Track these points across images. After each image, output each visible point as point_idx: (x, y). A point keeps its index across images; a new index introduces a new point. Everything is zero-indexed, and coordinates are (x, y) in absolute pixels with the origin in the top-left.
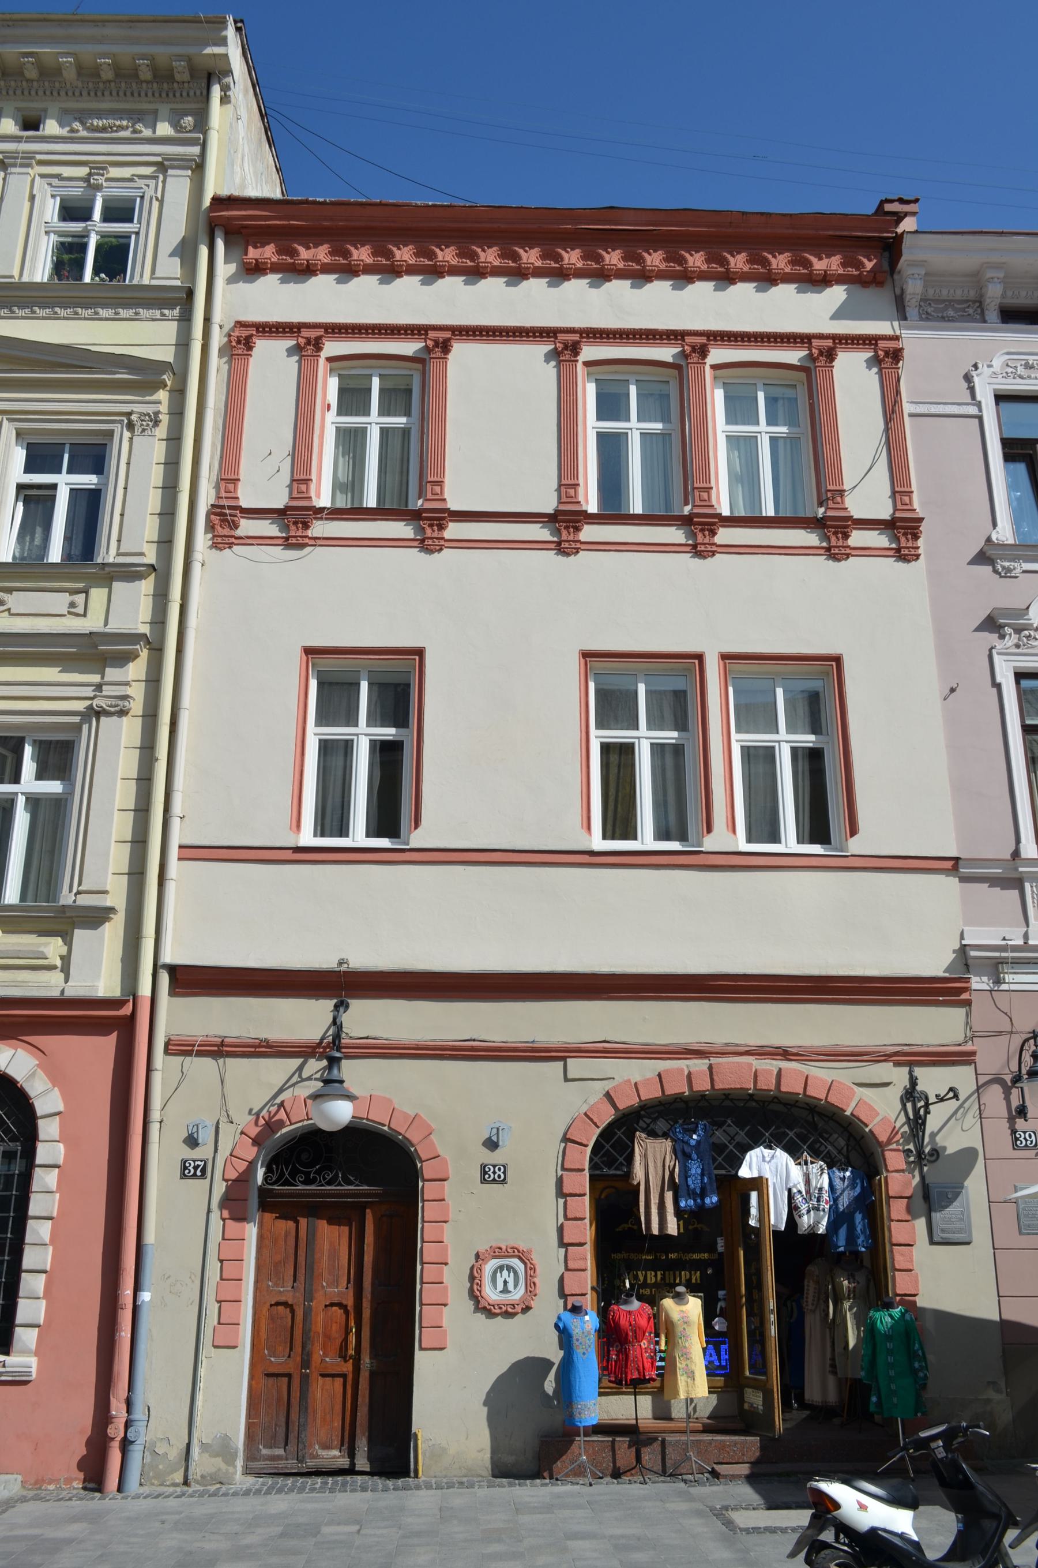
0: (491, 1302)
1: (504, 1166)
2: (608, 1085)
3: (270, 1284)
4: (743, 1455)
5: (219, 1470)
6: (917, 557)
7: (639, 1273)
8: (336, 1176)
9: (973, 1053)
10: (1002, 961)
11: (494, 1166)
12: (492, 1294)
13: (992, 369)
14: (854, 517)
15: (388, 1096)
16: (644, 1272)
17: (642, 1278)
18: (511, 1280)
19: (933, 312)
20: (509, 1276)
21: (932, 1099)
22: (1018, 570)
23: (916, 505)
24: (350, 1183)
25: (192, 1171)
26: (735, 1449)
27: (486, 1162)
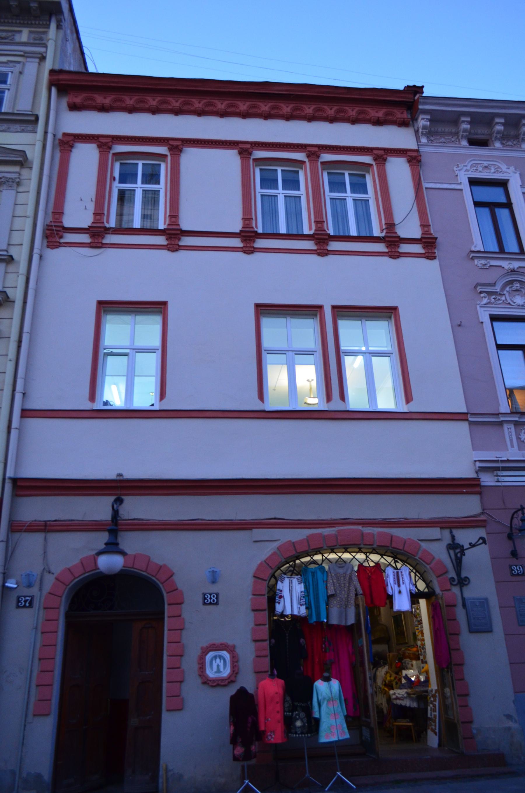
1: (216, 594)
2: (276, 545)
6: (435, 258)
9: (485, 521)
10: (497, 469)
11: (210, 595)
12: (211, 673)
13: (465, 168)
14: (401, 237)
18: (222, 664)
19: (434, 139)
21: (466, 546)
22: (488, 265)
23: (432, 232)
25: (23, 603)
27: (206, 592)
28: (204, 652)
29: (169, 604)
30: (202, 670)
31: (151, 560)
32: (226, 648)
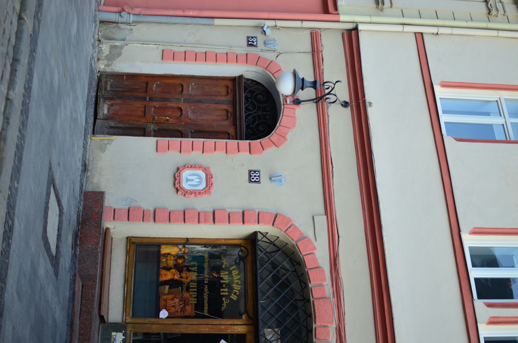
0: (181, 173)
2: (312, 237)
3: (193, 84)
4: (86, 300)
5: (103, 53)
7: (196, 268)
8: (250, 110)
11: (259, 176)
12: (186, 174)
15: (296, 125)
16: (196, 270)
17: (192, 269)
18: (193, 183)
20: (196, 182)
24: (247, 117)
26: (90, 296)
27: (261, 172)
28: (205, 169)
29: (249, 143)
30: (189, 167)
31: (291, 130)
32: (208, 188)
